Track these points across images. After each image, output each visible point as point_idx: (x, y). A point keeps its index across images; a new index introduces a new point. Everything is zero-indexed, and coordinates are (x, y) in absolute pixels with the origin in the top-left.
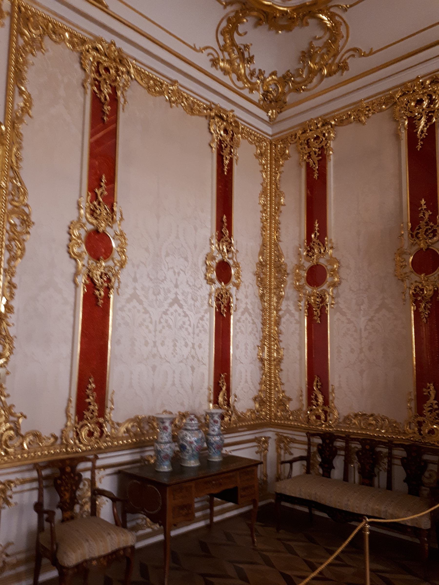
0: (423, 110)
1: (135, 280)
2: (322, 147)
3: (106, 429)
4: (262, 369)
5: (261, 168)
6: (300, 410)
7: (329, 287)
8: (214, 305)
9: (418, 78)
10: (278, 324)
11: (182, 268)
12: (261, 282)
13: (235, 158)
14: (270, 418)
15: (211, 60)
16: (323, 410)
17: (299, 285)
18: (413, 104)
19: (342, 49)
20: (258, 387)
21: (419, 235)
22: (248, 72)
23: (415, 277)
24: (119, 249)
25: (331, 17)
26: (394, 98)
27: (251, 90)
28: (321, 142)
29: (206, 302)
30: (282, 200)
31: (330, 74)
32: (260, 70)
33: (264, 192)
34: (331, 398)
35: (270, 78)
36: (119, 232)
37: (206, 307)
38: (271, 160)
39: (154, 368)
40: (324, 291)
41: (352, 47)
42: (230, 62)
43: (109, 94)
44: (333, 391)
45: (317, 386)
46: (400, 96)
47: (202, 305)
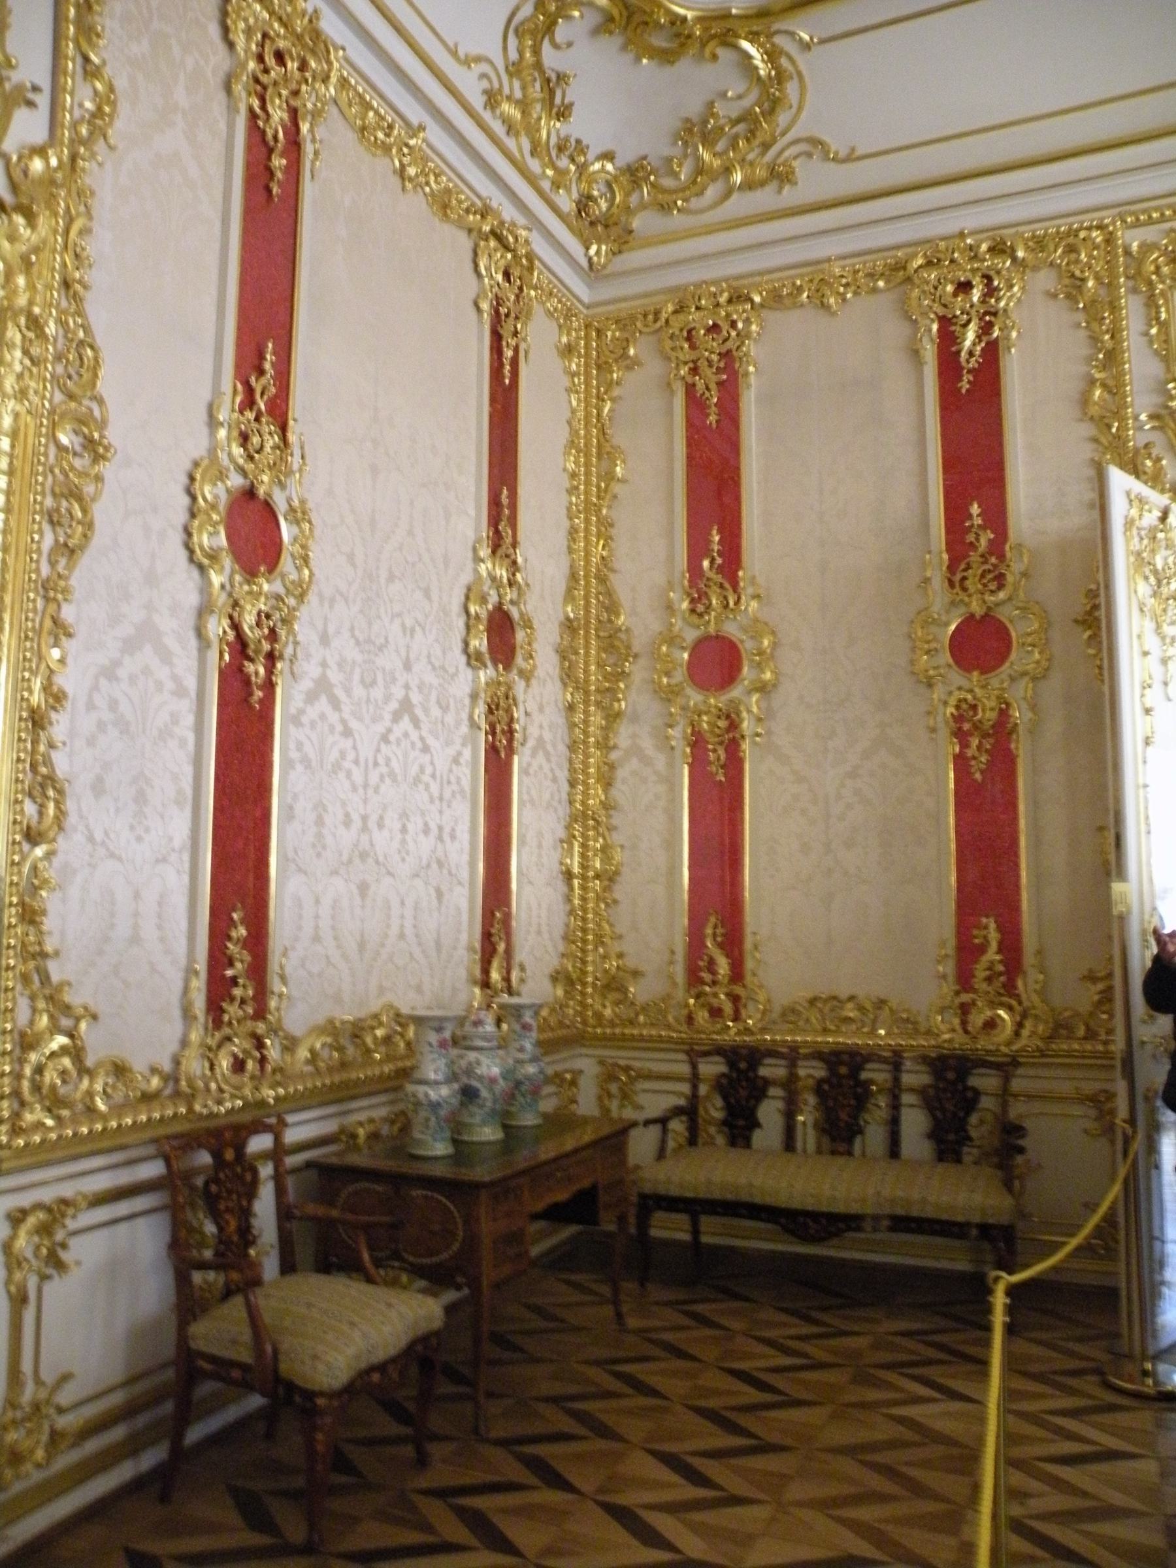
0: (972, 306)
1: (325, 640)
2: (729, 352)
3: (273, 1052)
4: (568, 899)
5: (566, 381)
6: (667, 998)
7: (749, 692)
8: (484, 725)
9: (962, 235)
10: (608, 784)
11: (420, 617)
12: (568, 676)
13: (523, 346)
14: (585, 1022)
15: (485, 92)
16: (727, 995)
17: (669, 685)
18: (950, 288)
19: (783, 134)
20: (561, 948)
21: (968, 583)
22: (553, 140)
23: (957, 677)
24: (297, 549)
25: (772, 56)
26: (904, 268)
27: (556, 185)
28: (726, 340)
29: (464, 716)
30: (618, 469)
31: (749, 185)
32: (578, 142)
33: (572, 444)
34: (749, 964)
35: (597, 166)
36: (296, 503)
37: (465, 729)
38: (587, 365)
39: (363, 888)
40: (735, 705)
41: (804, 134)
42: (524, 105)
43: (284, 127)
44: (756, 947)
45: (715, 935)
46: (920, 267)
47: (458, 723)
